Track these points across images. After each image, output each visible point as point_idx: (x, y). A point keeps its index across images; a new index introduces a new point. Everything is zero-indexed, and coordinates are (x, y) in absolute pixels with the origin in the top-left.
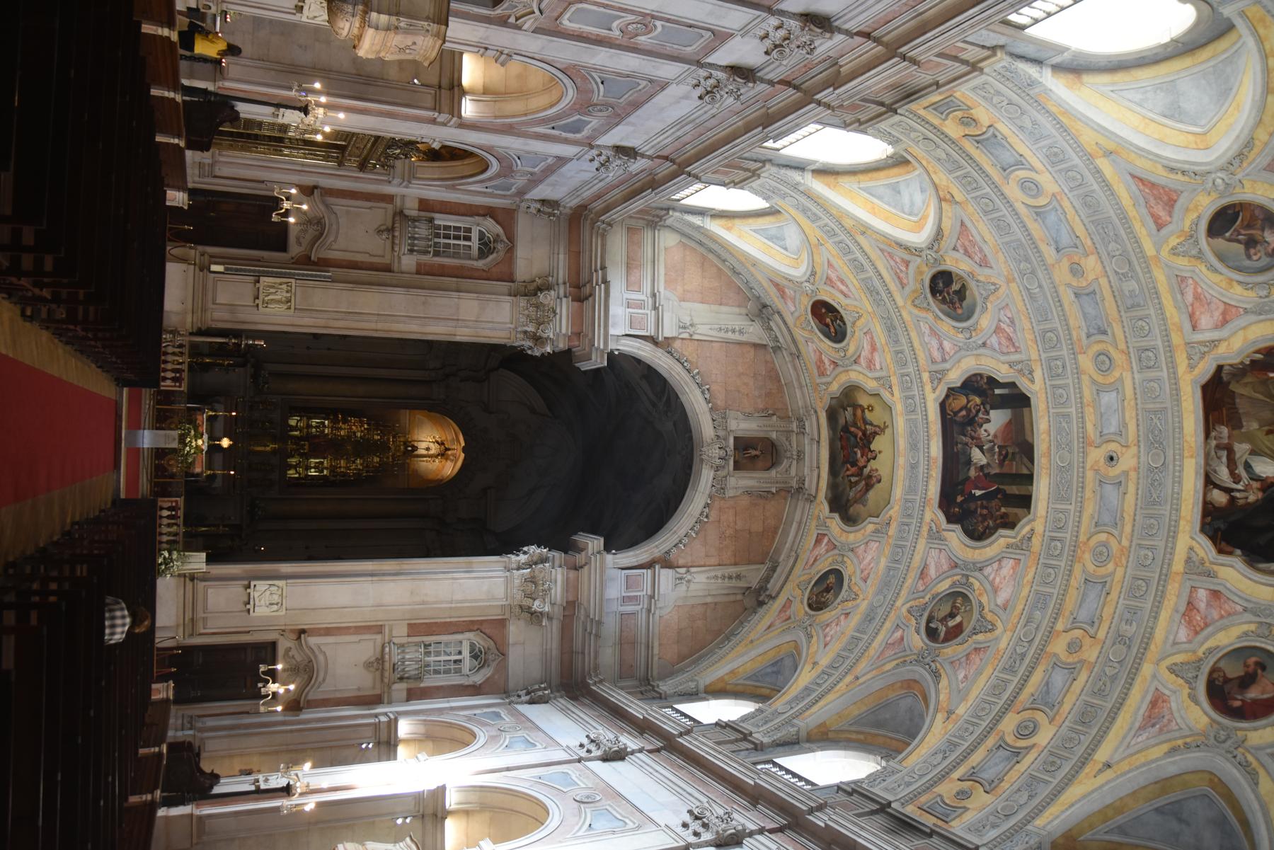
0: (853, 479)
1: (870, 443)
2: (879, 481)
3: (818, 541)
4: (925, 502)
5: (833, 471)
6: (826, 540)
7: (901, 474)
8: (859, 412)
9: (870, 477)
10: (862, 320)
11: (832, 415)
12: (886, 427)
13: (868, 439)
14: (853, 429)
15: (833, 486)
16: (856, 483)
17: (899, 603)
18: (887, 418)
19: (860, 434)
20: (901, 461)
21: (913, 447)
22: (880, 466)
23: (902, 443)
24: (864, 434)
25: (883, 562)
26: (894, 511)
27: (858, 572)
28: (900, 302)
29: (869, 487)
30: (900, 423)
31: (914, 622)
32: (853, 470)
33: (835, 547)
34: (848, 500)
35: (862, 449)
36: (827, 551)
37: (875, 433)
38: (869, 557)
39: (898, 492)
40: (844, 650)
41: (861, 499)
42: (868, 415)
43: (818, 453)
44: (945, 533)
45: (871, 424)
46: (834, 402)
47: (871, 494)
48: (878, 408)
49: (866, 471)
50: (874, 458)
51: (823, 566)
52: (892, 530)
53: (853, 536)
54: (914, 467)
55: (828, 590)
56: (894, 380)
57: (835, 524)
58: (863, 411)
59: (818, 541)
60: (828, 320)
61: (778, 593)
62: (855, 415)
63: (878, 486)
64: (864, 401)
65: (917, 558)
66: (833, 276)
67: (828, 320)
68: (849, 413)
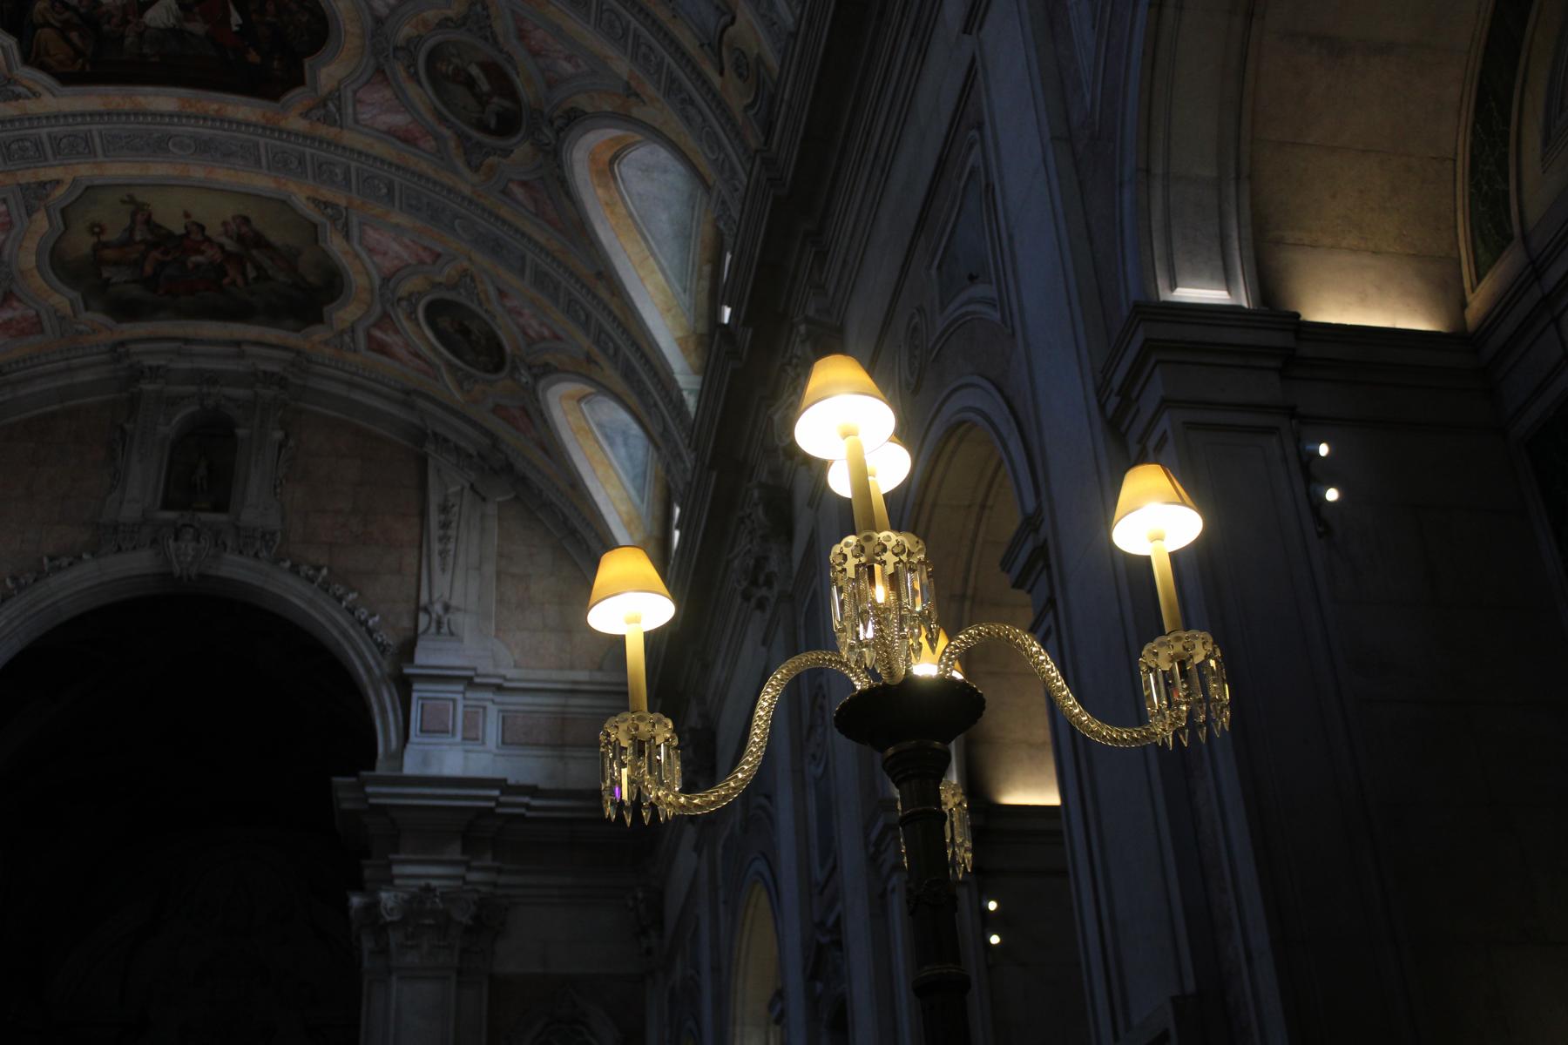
0: (252, 273)
1: (170, 235)
2: (246, 220)
3: (382, 349)
6: (378, 333)
7: (223, 175)
9: (240, 239)
13: (161, 239)
14: (148, 269)
16: (258, 267)
17: (467, 190)
19: (156, 254)
22: (215, 216)
25: (398, 218)
29: (260, 242)
30: (120, 170)
31: (492, 159)
33: (385, 315)
36: (397, 332)
37: (148, 221)
38: (396, 247)
39: (262, 182)
42: (112, 235)
45: (131, 230)
47: (274, 237)
49: (230, 245)
50: (202, 228)
51: (424, 338)
53: (357, 280)
54: (203, 148)
55: (466, 332)
57: (345, 314)
58: (106, 245)
59: (382, 349)
61: (487, 433)
64: (83, 243)
65: (379, 149)
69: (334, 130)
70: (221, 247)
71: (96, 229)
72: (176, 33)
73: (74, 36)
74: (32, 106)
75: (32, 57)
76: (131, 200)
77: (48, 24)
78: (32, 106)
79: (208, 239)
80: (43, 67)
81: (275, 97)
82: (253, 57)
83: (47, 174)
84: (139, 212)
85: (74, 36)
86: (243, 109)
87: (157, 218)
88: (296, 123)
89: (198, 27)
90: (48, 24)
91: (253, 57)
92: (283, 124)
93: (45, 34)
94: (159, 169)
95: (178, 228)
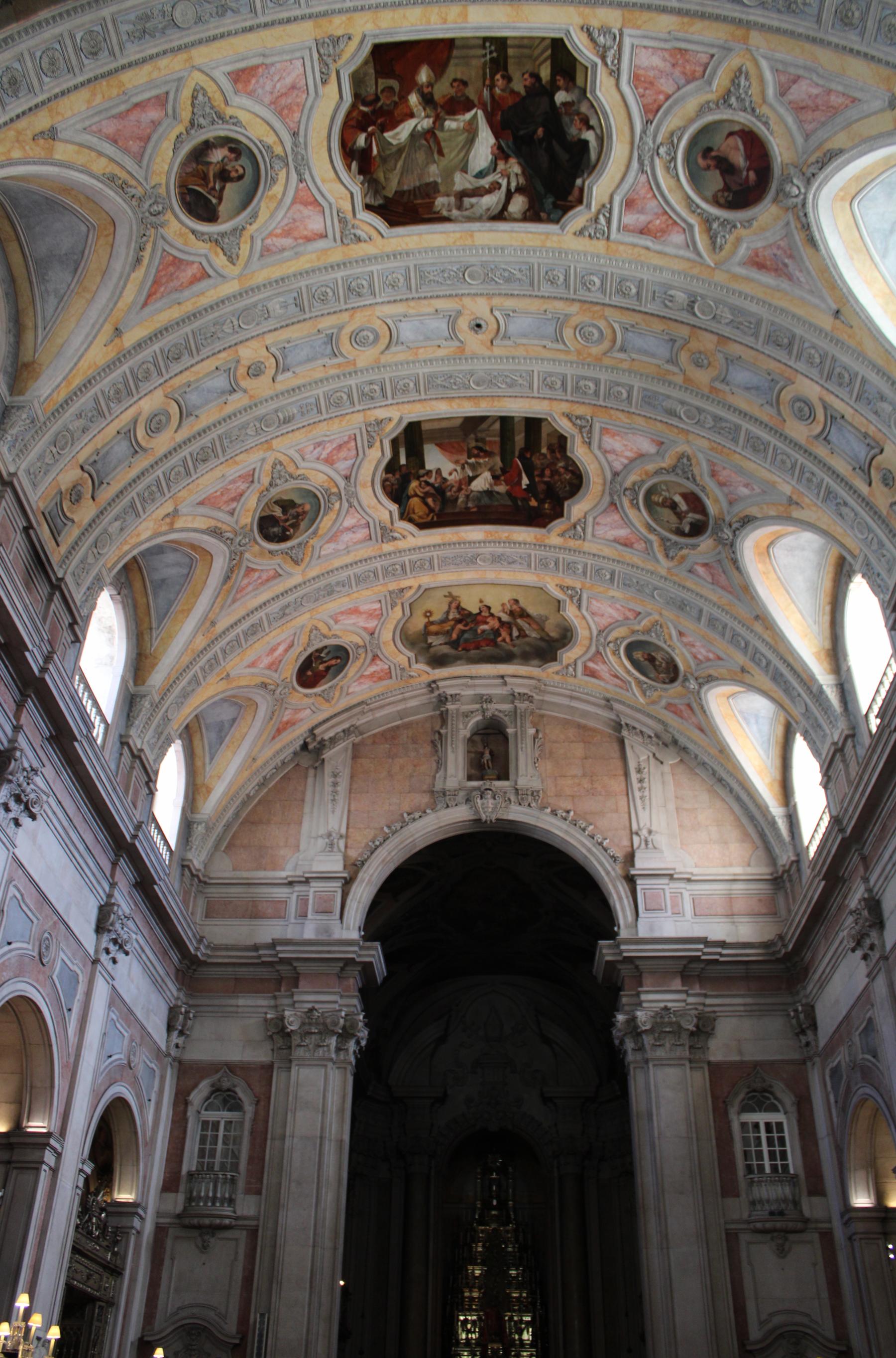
1: (470, 614)
2: (516, 601)
3: (592, 674)
5: (507, 658)
6: (591, 665)
7: (507, 575)
8: (433, 628)
9: (511, 613)
11: (438, 661)
13: (466, 617)
15: (525, 658)
16: (520, 630)
18: (440, 594)
19: (460, 626)
20: (490, 576)
22: (498, 601)
24: (459, 621)
29: (524, 614)
30: (445, 577)
32: (504, 634)
34: (542, 639)
35: (478, 623)
37: (458, 607)
38: (610, 610)
39: (529, 578)
40: (723, 635)
41: (539, 623)
42: (436, 617)
43: (485, 677)
45: (448, 613)
48: (429, 605)
49: (505, 618)
50: (489, 608)
56: (393, 586)
58: (432, 623)
59: (592, 674)
62: (436, 634)
63: (522, 603)
64: (419, 623)
70: (499, 619)
71: (428, 614)
72: (489, 493)
74: (401, 544)
75: (405, 516)
76: (450, 595)
77: (416, 495)
78: (401, 544)
79: (492, 615)
80: (411, 520)
82: (533, 503)
83: (405, 583)
84: (454, 601)
85: (430, 501)
86: (523, 534)
87: (463, 605)
90: (416, 495)
91: (533, 503)
92: (547, 541)
94: (468, 575)
95: (475, 611)
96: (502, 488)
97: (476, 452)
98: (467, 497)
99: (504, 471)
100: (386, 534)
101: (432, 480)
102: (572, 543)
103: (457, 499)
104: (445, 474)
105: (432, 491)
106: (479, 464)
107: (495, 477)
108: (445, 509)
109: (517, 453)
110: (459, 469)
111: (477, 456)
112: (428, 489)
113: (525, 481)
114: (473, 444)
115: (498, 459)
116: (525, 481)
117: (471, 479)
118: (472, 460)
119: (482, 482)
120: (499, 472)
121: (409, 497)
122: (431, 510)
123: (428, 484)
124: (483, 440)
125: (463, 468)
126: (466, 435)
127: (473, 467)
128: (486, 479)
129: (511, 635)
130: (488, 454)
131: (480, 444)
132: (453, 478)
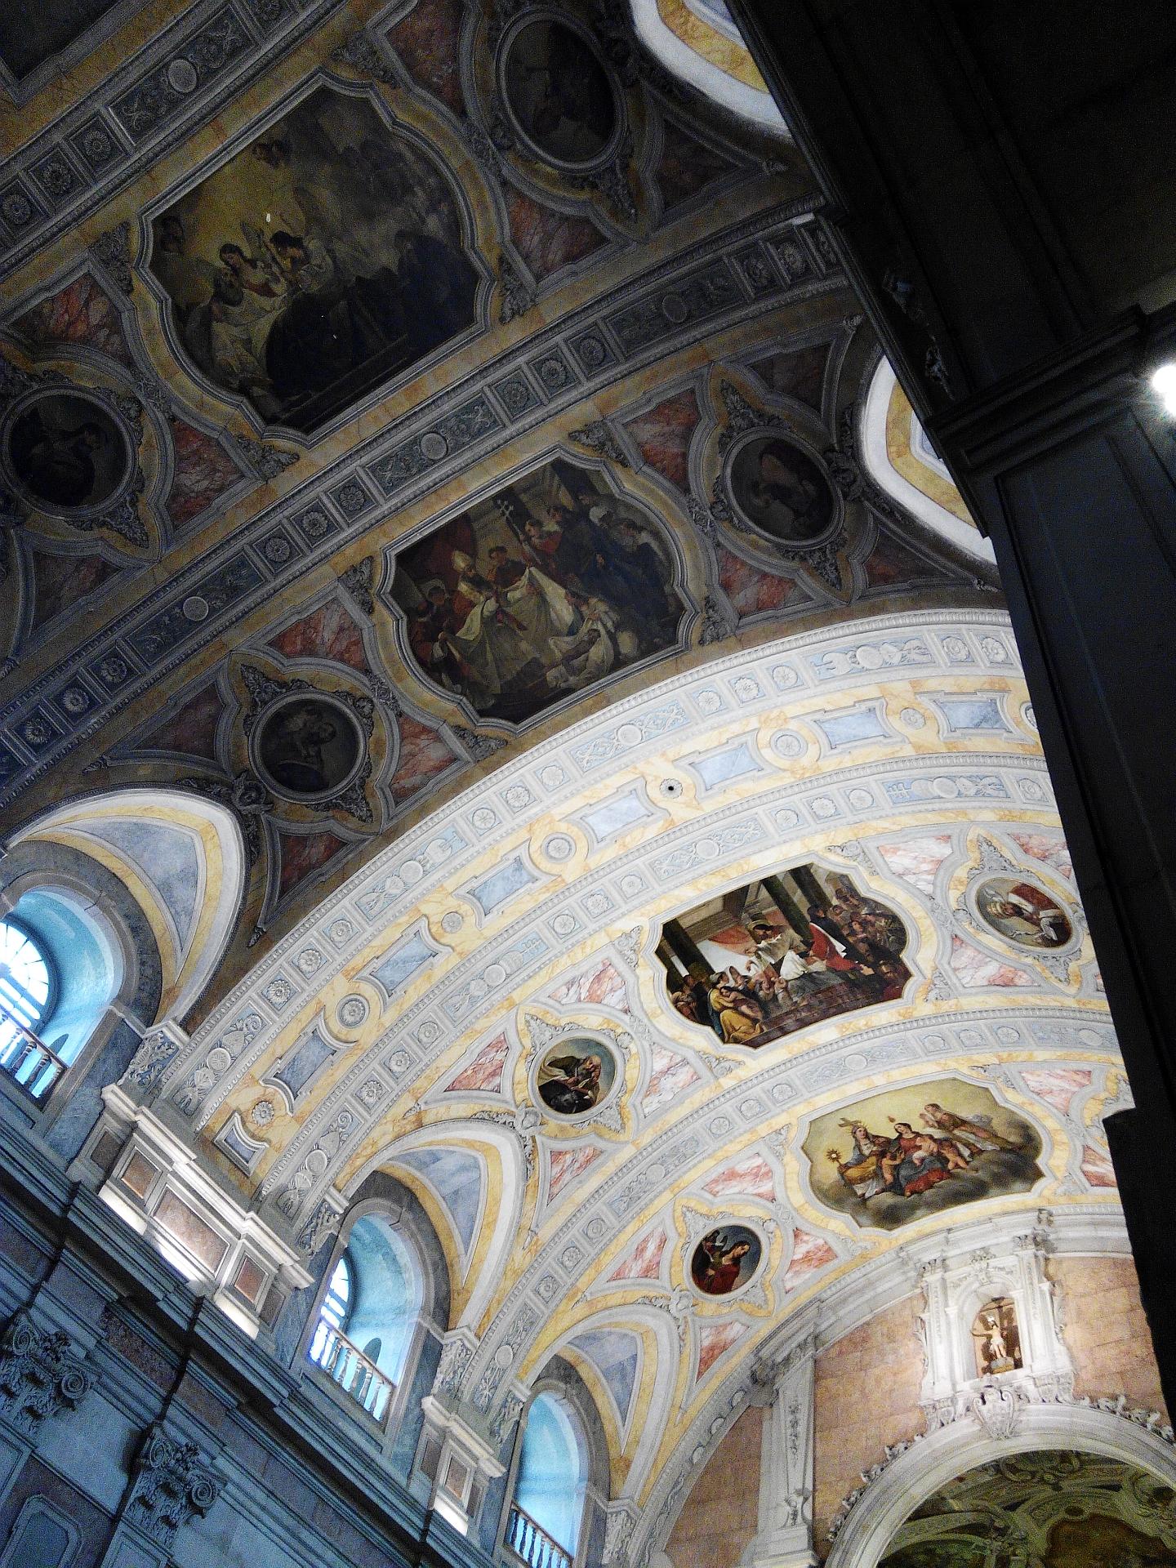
4: (910, 1022)
10: (692, 1204)
12: (845, 1123)
21: (841, 1069)
23: (853, 1089)
26: (959, 1065)
27: (1087, 1090)
28: (628, 1152)
44: (928, 974)
46: (863, 1220)
52: (986, 1058)
60: (725, 1261)
66: (637, 1268)
67: (725, 1261)
68: (869, 1189)
69: (952, 1002)
72: (807, 977)
73: (744, 1008)
77: (725, 1008)
81: (898, 995)
82: (867, 971)
85: (744, 1008)
86: (881, 1014)
88: (925, 1009)
89: (819, 966)
90: (725, 1008)
91: (867, 971)
92: (916, 1014)
93: (726, 1015)
96: (819, 966)
97: (761, 932)
98: (785, 989)
99: (809, 945)
100: (716, 1066)
101: (732, 984)
102: (947, 1006)
103: (775, 996)
104: (744, 972)
105: (741, 997)
106: (774, 945)
107: (803, 955)
108: (764, 1015)
109: (808, 918)
110: (754, 959)
111: (765, 937)
112: (733, 995)
113: (840, 948)
114: (752, 925)
115: (791, 932)
116: (840, 948)
117: (777, 967)
118: (763, 944)
119: (792, 967)
120: (803, 948)
121: (718, 1014)
122: (755, 1021)
123: (730, 989)
124: (764, 917)
125: (759, 957)
126: (737, 916)
127: (769, 951)
128: (793, 961)
129: (960, 1155)
130: (777, 930)
131: (760, 922)
132: (755, 972)
